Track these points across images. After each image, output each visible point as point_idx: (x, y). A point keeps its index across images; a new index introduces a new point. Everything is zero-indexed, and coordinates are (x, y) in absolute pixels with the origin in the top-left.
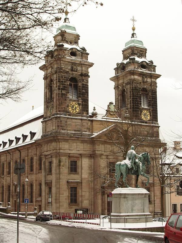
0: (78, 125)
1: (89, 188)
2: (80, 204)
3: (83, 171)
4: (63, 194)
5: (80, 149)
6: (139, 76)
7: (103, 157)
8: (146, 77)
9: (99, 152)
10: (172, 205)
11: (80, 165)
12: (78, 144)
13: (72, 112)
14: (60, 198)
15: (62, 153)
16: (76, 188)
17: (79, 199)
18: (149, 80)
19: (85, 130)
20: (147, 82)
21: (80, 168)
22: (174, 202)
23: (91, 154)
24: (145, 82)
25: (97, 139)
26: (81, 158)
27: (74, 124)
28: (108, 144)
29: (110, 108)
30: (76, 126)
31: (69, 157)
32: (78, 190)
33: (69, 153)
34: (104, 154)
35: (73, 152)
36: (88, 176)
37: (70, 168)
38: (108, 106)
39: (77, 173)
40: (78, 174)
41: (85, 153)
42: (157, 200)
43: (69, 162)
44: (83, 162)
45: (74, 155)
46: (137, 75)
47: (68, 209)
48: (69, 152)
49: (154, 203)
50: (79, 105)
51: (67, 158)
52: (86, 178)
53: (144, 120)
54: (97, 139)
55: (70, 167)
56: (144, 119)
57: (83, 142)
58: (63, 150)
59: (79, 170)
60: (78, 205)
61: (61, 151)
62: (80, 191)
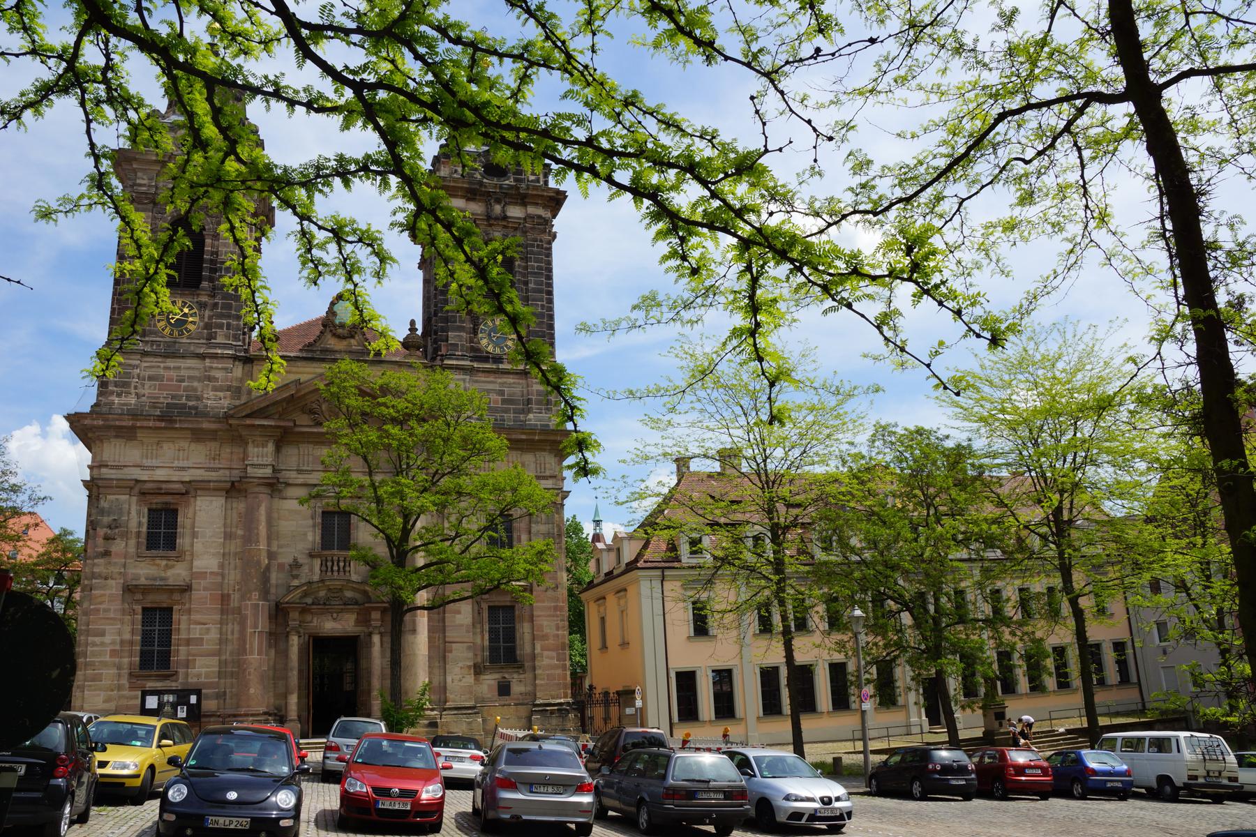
0: (191, 378)
1: (223, 612)
2: (182, 671)
3: (198, 546)
4: (102, 634)
5: (185, 464)
6: (468, 199)
7: (291, 492)
8: (498, 201)
9: (261, 471)
10: (673, 675)
11: (188, 522)
12: (184, 444)
13: (167, 330)
14: (89, 648)
15: (105, 479)
16: (170, 610)
17: (180, 653)
18: (515, 212)
19: (218, 393)
20: (505, 218)
21: (188, 531)
22: (681, 662)
23: (233, 483)
24: (496, 219)
25: (248, 416)
26: (195, 497)
27: (173, 374)
28: (317, 443)
29: (334, 314)
30: (183, 381)
31: (143, 494)
32: (175, 617)
33: (145, 478)
34: (300, 481)
35: (160, 475)
36: (222, 566)
37: (144, 535)
38: (333, 304)
39: (172, 553)
40: (179, 558)
41: (213, 475)
42: (546, 653)
43: (139, 513)
44: (202, 518)
45: (164, 486)
46: (462, 197)
47: (126, 693)
48: (144, 475)
49: (534, 668)
50: (200, 310)
51: (134, 499)
52: (212, 573)
53: (487, 352)
54: (248, 416)
55: (144, 529)
56: (490, 349)
57: (198, 436)
58: (113, 467)
59: (183, 541)
60: (173, 676)
61: (104, 470)
62: (183, 626)
